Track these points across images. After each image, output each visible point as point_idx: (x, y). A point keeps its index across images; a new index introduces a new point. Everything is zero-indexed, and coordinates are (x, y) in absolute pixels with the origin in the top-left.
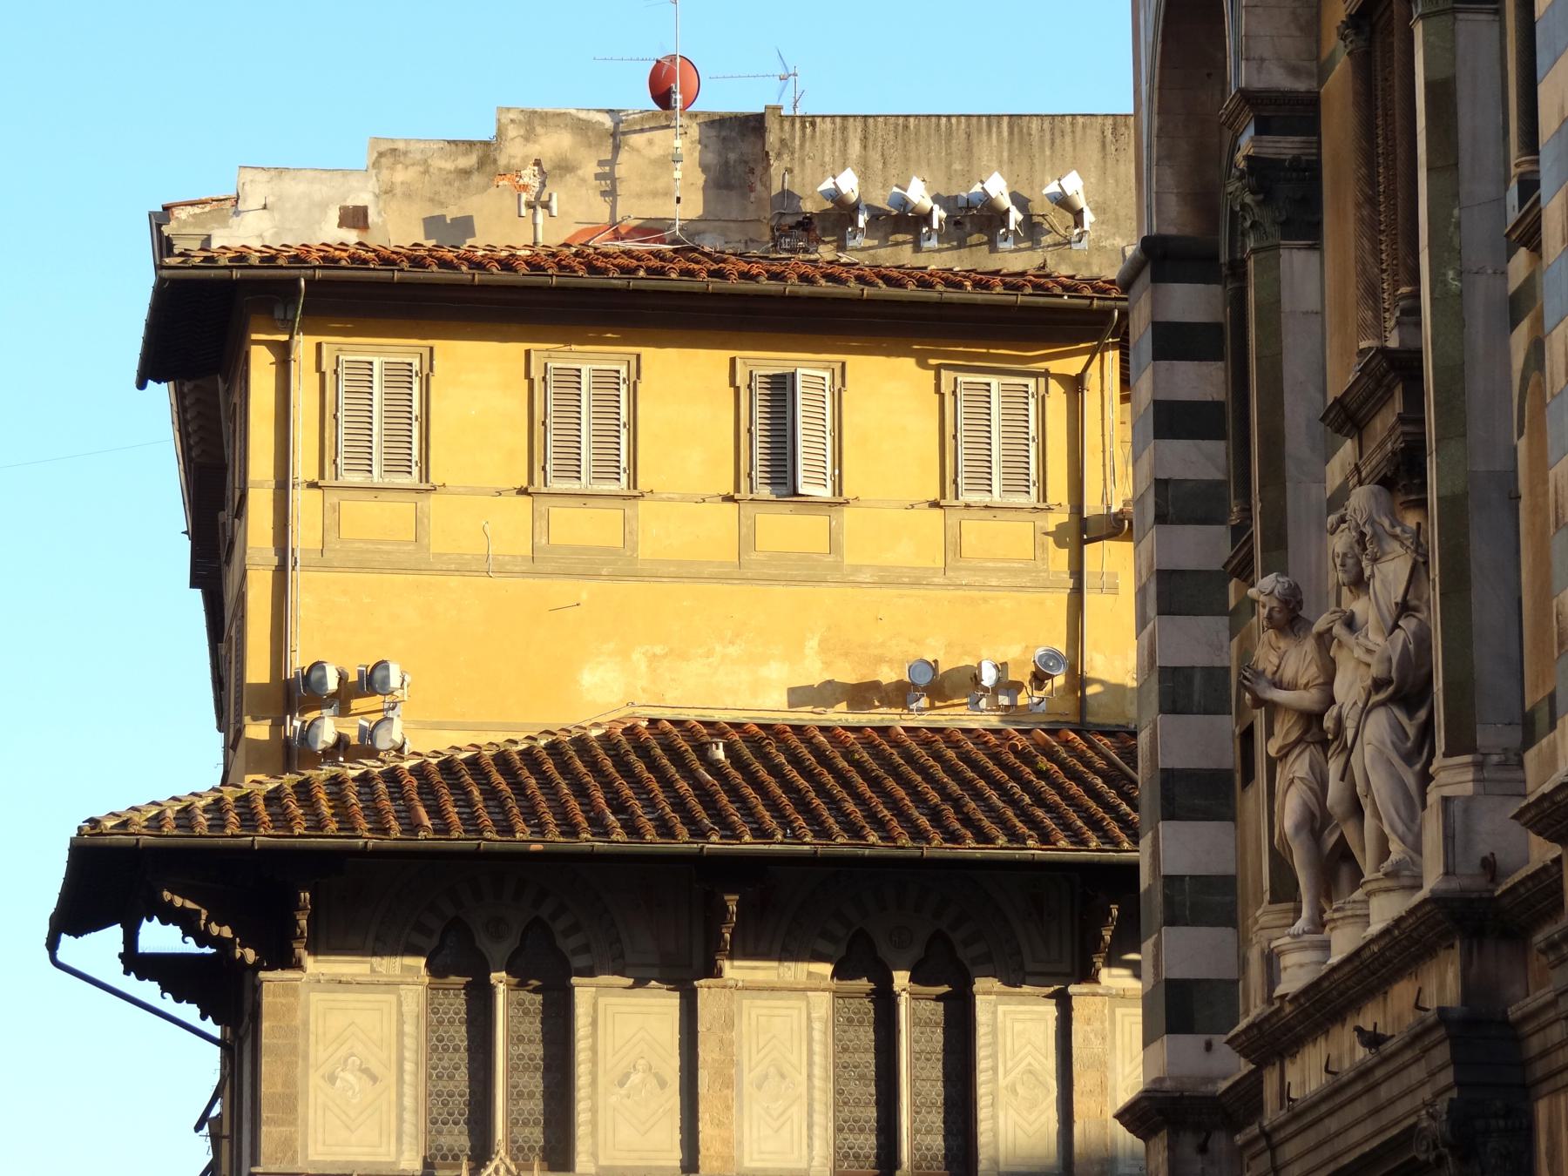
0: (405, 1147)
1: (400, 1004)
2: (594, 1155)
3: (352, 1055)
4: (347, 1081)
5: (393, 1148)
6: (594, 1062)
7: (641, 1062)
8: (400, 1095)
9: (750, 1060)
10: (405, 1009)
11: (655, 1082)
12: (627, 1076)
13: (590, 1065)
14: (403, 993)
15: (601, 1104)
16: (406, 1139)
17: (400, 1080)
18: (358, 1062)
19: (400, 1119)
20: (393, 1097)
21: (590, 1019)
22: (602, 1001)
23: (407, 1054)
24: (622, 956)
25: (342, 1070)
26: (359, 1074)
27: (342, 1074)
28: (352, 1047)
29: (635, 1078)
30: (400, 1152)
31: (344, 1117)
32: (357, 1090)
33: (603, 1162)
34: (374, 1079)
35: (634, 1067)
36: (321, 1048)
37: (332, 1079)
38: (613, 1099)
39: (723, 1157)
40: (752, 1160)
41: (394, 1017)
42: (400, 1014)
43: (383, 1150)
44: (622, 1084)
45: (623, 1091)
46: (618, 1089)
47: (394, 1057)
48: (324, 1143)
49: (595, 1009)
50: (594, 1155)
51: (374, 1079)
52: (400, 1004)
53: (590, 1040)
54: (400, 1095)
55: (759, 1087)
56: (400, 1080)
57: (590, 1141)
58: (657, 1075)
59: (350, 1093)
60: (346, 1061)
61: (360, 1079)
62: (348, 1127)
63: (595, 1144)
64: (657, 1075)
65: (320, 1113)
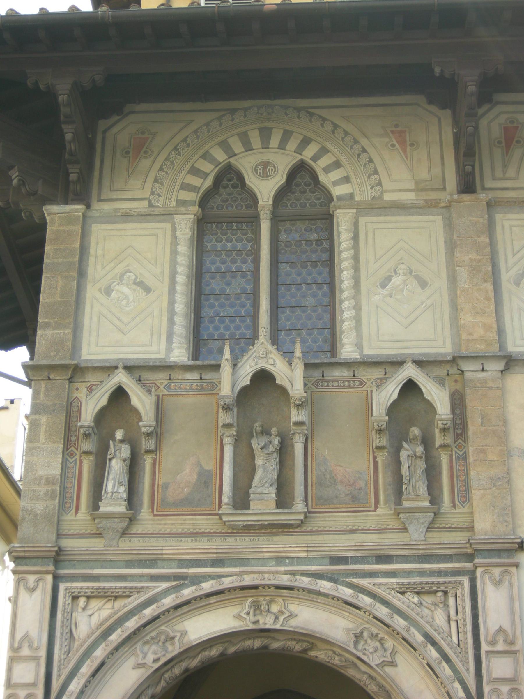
0: (175, 345)
1: (174, 230)
2: (359, 346)
3: (129, 271)
4: (122, 293)
5: (163, 346)
6: (356, 268)
7: (403, 266)
8: (172, 302)
9: (506, 262)
10: (179, 233)
11: (415, 283)
12: (389, 279)
13: (352, 271)
14: (177, 221)
15: (364, 302)
16: (176, 339)
17: (172, 291)
18: (133, 277)
19: (171, 322)
20: (165, 304)
21: (351, 235)
22: (362, 220)
23: (179, 269)
24: (380, 184)
25: (118, 284)
26: (134, 287)
27: (117, 287)
28: (127, 266)
29: (397, 280)
30: (169, 350)
31: (118, 323)
32: (131, 299)
33: (367, 351)
34: (148, 290)
35: (395, 271)
36: (99, 267)
37: (108, 291)
38: (376, 298)
39: (486, 341)
40: (515, 345)
41: (168, 241)
42: (174, 237)
43: (154, 348)
44: (383, 286)
45: (385, 291)
46: (380, 290)
47: (167, 271)
48: (97, 345)
49: (356, 224)
50: (359, 346)
51: (148, 290)
52: (174, 230)
53: (352, 251)
54: (172, 302)
55: (517, 284)
56: (172, 291)
57: (355, 334)
58: (417, 278)
59: (124, 302)
60: (122, 276)
61: (134, 290)
62: (120, 330)
63: (359, 336)
64: (417, 278)
65: (95, 319)
